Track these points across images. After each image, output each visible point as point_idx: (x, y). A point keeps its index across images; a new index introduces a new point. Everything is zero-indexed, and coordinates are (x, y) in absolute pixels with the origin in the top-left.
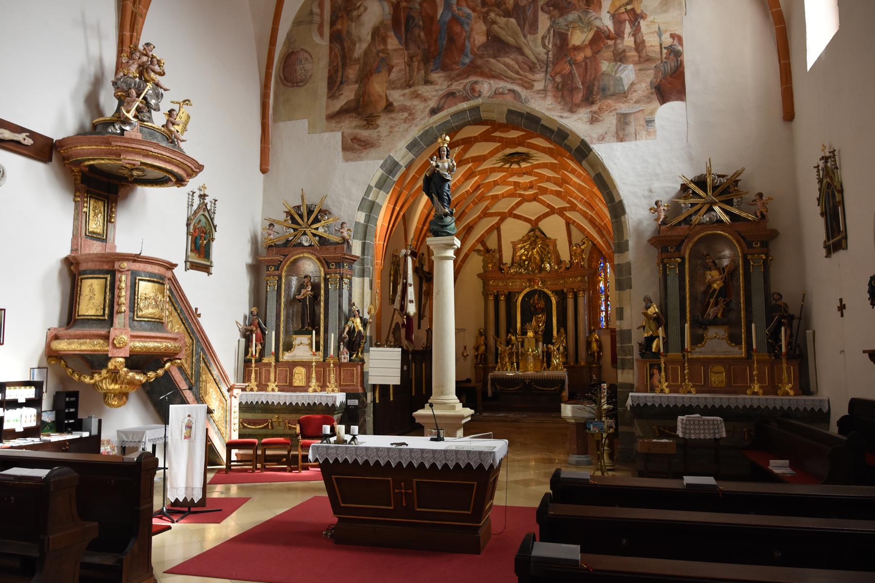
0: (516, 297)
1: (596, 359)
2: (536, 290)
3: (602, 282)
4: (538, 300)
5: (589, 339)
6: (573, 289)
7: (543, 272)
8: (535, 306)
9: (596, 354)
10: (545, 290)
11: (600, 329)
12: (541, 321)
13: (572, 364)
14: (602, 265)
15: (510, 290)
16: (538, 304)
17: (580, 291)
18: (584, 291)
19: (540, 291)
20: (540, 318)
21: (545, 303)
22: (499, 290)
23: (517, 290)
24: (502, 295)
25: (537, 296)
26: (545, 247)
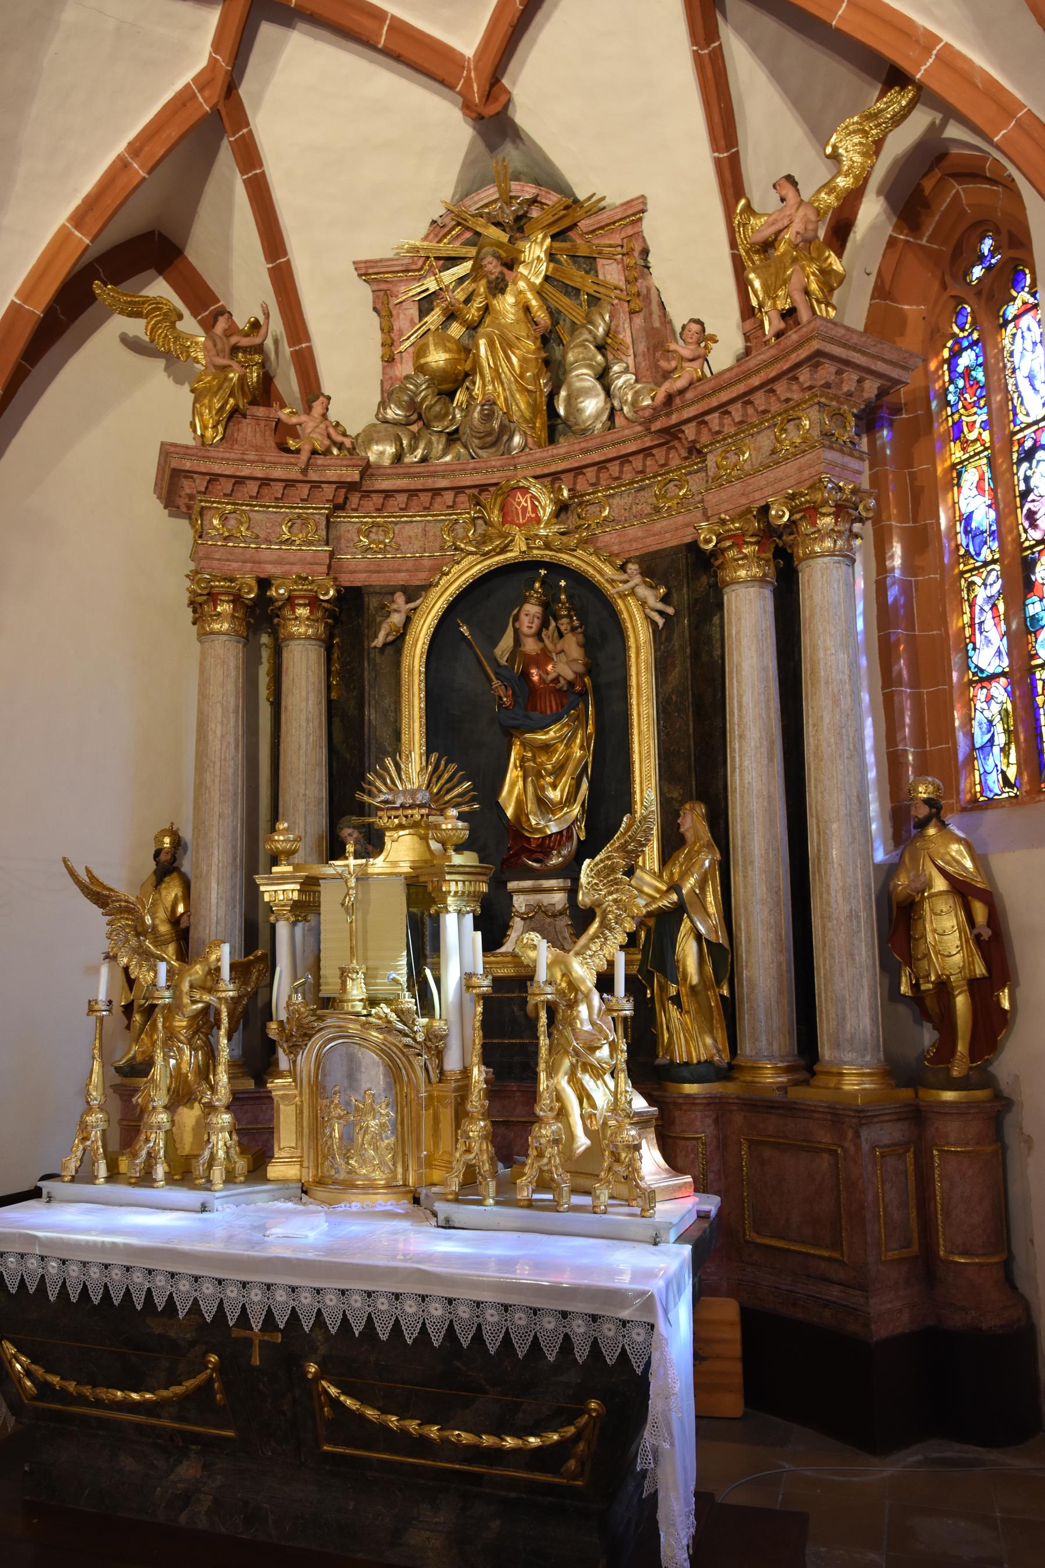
0: (397, 619)
1: (962, 1047)
2: (525, 568)
3: (970, 477)
4: (538, 636)
5: (902, 881)
6: (765, 509)
7: (563, 446)
8: (525, 675)
9: (961, 1001)
10: (577, 560)
11: (976, 806)
12: (558, 771)
13: (770, 1077)
14: (967, 359)
15: (359, 580)
16: (543, 658)
17: (812, 511)
18: (841, 510)
19: (557, 569)
20: (547, 748)
21: (589, 646)
22: (270, 570)
23: (401, 578)
24: (290, 601)
25: (532, 610)
26: (577, 277)
